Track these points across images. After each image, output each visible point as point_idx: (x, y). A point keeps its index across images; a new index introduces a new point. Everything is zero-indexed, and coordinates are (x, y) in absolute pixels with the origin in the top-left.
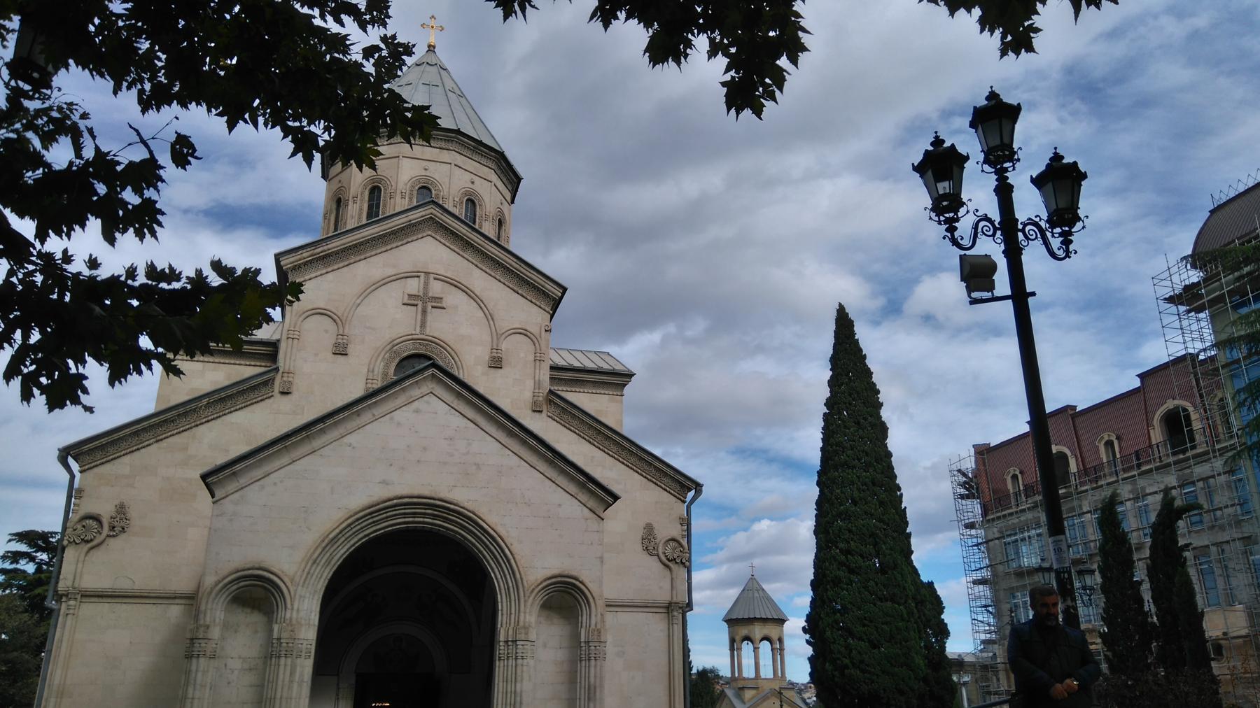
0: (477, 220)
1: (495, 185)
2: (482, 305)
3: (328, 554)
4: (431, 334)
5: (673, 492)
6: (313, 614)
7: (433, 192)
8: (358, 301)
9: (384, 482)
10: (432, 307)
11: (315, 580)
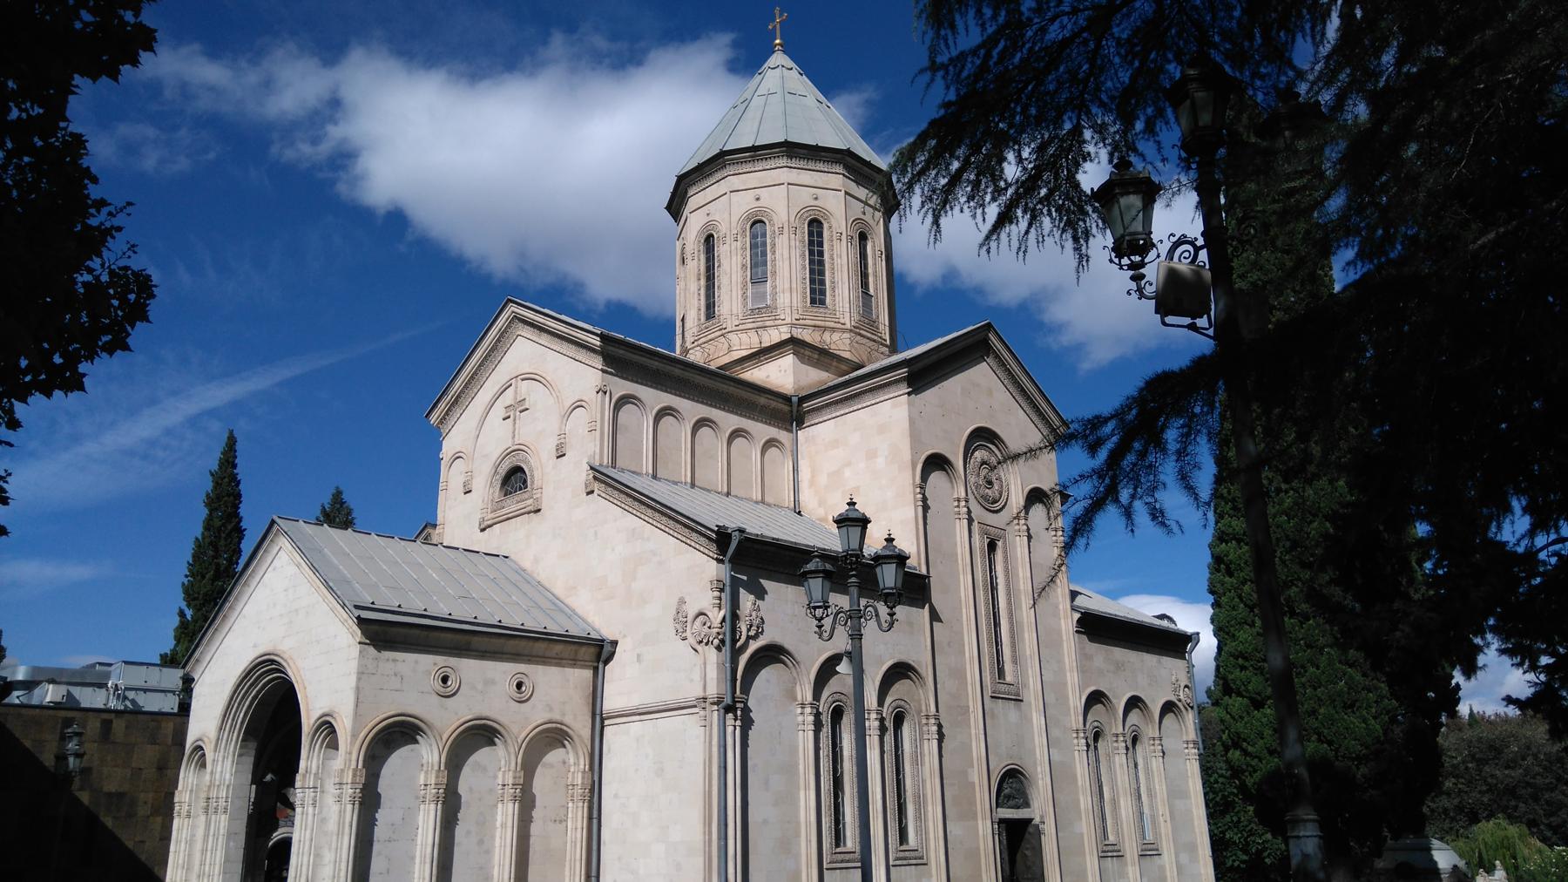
0: (768, 241)
1: (789, 184)
2: (551, 390)
3: (230, 721)
4: (520, 442)
5: (702, 549)
6: (228, 776)
7: (715, 236)
8: (477, 432)
9: (255, 646)
10: (521, 412)
11: (226, 744)
